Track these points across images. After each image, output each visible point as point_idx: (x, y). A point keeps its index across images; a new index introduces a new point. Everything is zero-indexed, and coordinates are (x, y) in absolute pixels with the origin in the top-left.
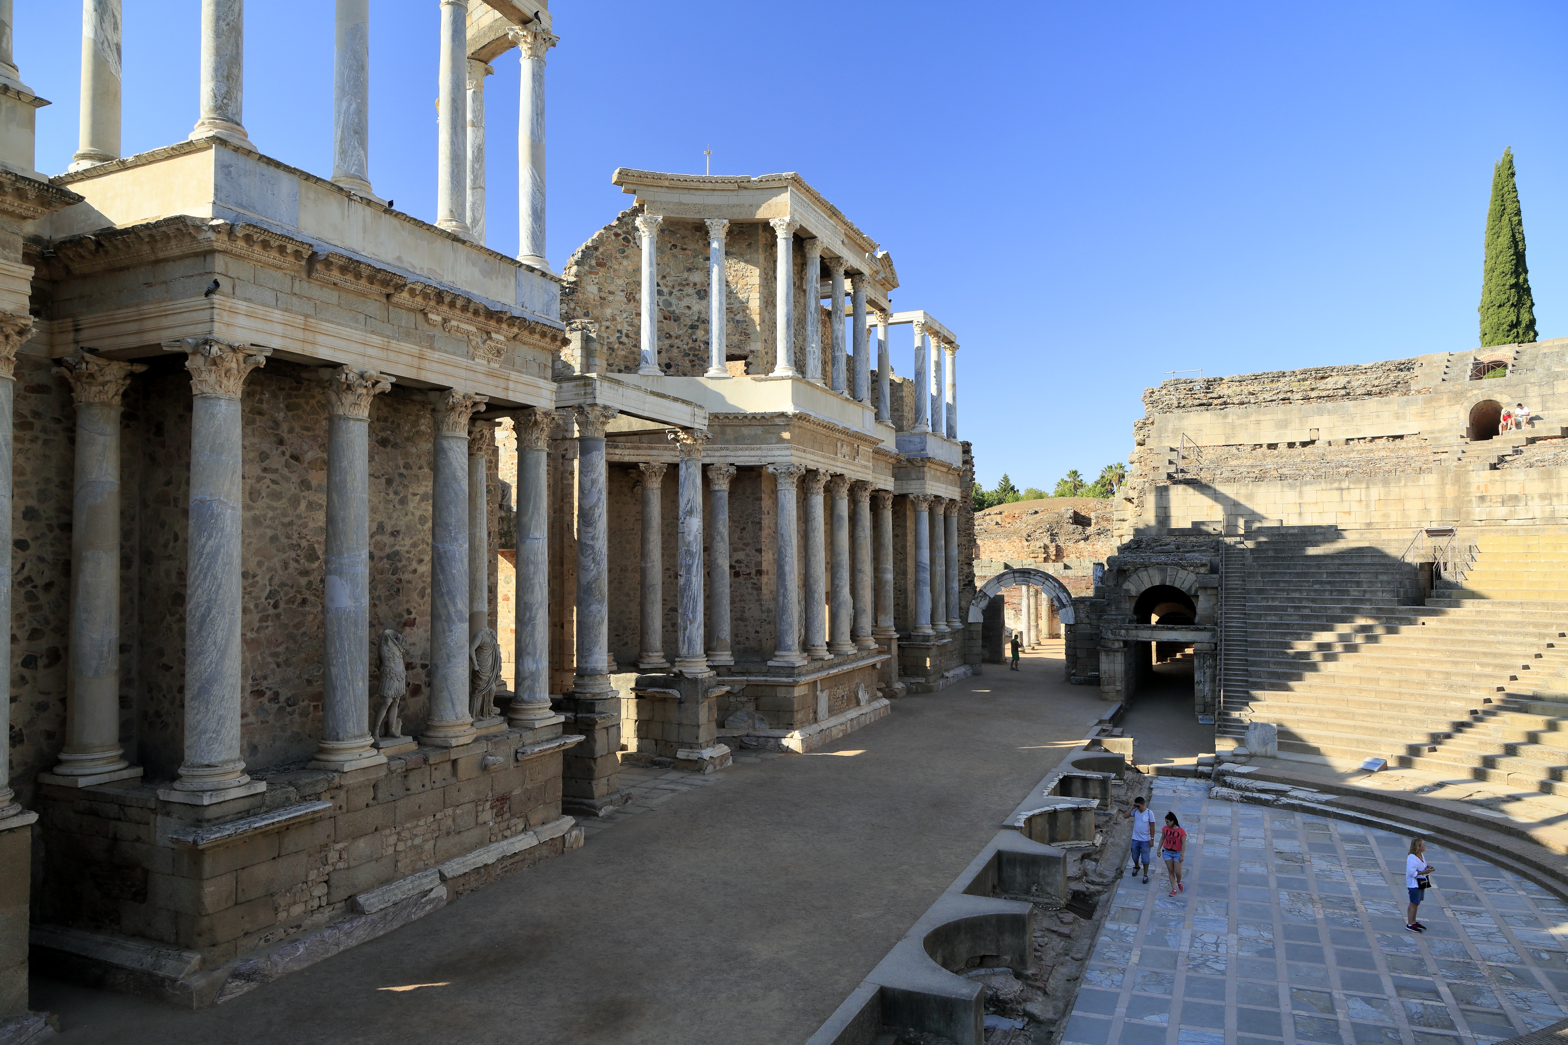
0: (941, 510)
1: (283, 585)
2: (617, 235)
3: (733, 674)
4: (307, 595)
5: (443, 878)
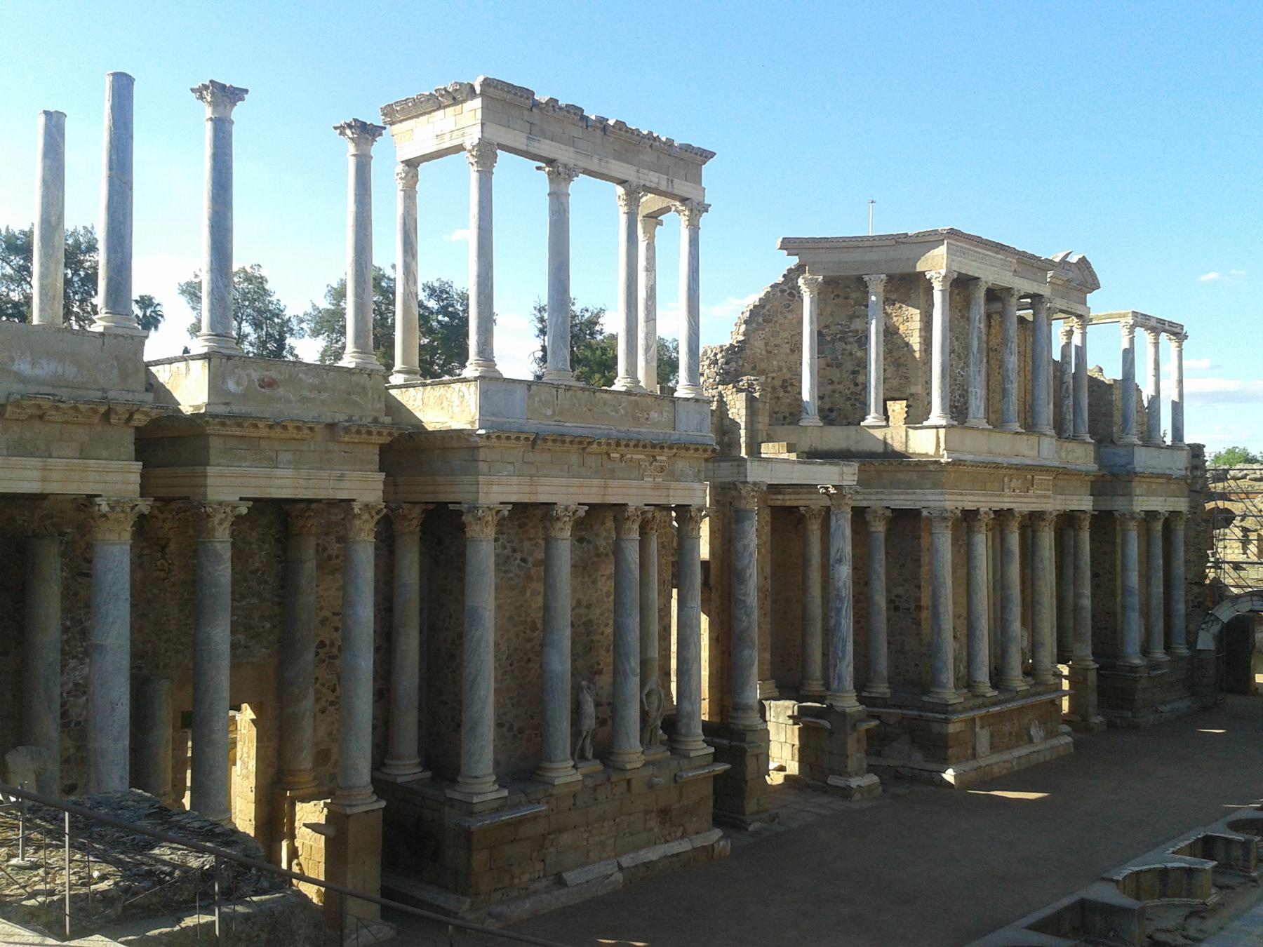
0: (1158, 526)
1: (516, 650)
2: (783, 291)
3: (889, 707)
4: (531, 655)
5: (620, 868)
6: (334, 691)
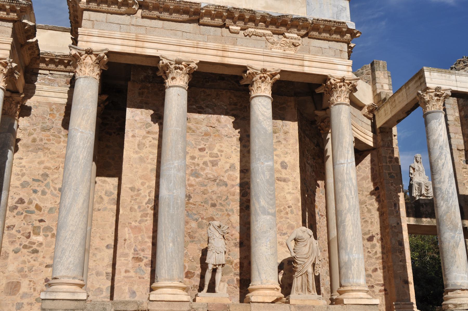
6: (28, 237)
